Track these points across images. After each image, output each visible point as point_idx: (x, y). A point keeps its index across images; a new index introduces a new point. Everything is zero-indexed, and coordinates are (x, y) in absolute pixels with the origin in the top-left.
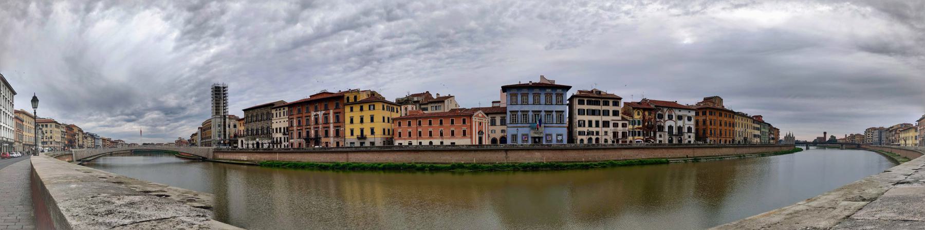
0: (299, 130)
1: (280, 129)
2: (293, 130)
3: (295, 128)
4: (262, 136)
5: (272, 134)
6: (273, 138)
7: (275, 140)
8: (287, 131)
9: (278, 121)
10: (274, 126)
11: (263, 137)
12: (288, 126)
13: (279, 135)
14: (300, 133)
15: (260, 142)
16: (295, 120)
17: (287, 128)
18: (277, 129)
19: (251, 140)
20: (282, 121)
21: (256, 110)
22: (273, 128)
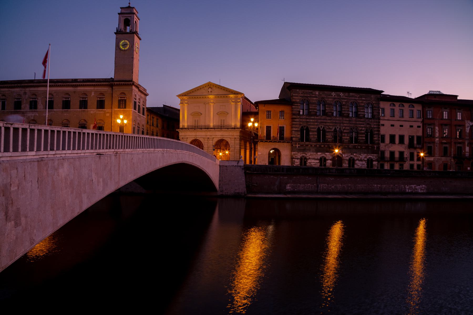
0: (445, 143)
1: (402, 138)
2: (434, 142)
3: (437, 140)
4: (351, 146)
5: (379, 144)
6: (383, 153)
7: (387, 155)
8: (418, 143)
9: (397, 124)
10: (386, 130)
11: (354, 147)
12: (420, 134)
13: (397, 148)
14: (446, 149)
15: (346, 157)
16: (437, 128)
17: (418, 138)
18: (392, 138)
19: (317, 151)
20: (407, 125)
21: (333, 94)
22: (382, 132)
